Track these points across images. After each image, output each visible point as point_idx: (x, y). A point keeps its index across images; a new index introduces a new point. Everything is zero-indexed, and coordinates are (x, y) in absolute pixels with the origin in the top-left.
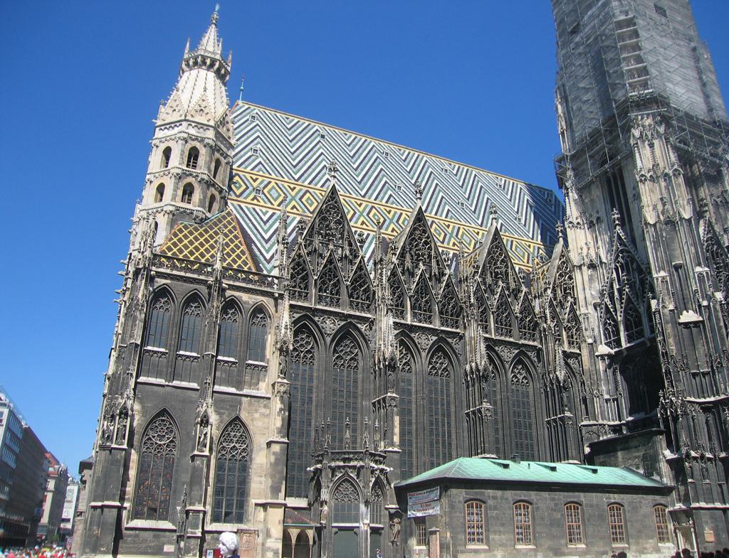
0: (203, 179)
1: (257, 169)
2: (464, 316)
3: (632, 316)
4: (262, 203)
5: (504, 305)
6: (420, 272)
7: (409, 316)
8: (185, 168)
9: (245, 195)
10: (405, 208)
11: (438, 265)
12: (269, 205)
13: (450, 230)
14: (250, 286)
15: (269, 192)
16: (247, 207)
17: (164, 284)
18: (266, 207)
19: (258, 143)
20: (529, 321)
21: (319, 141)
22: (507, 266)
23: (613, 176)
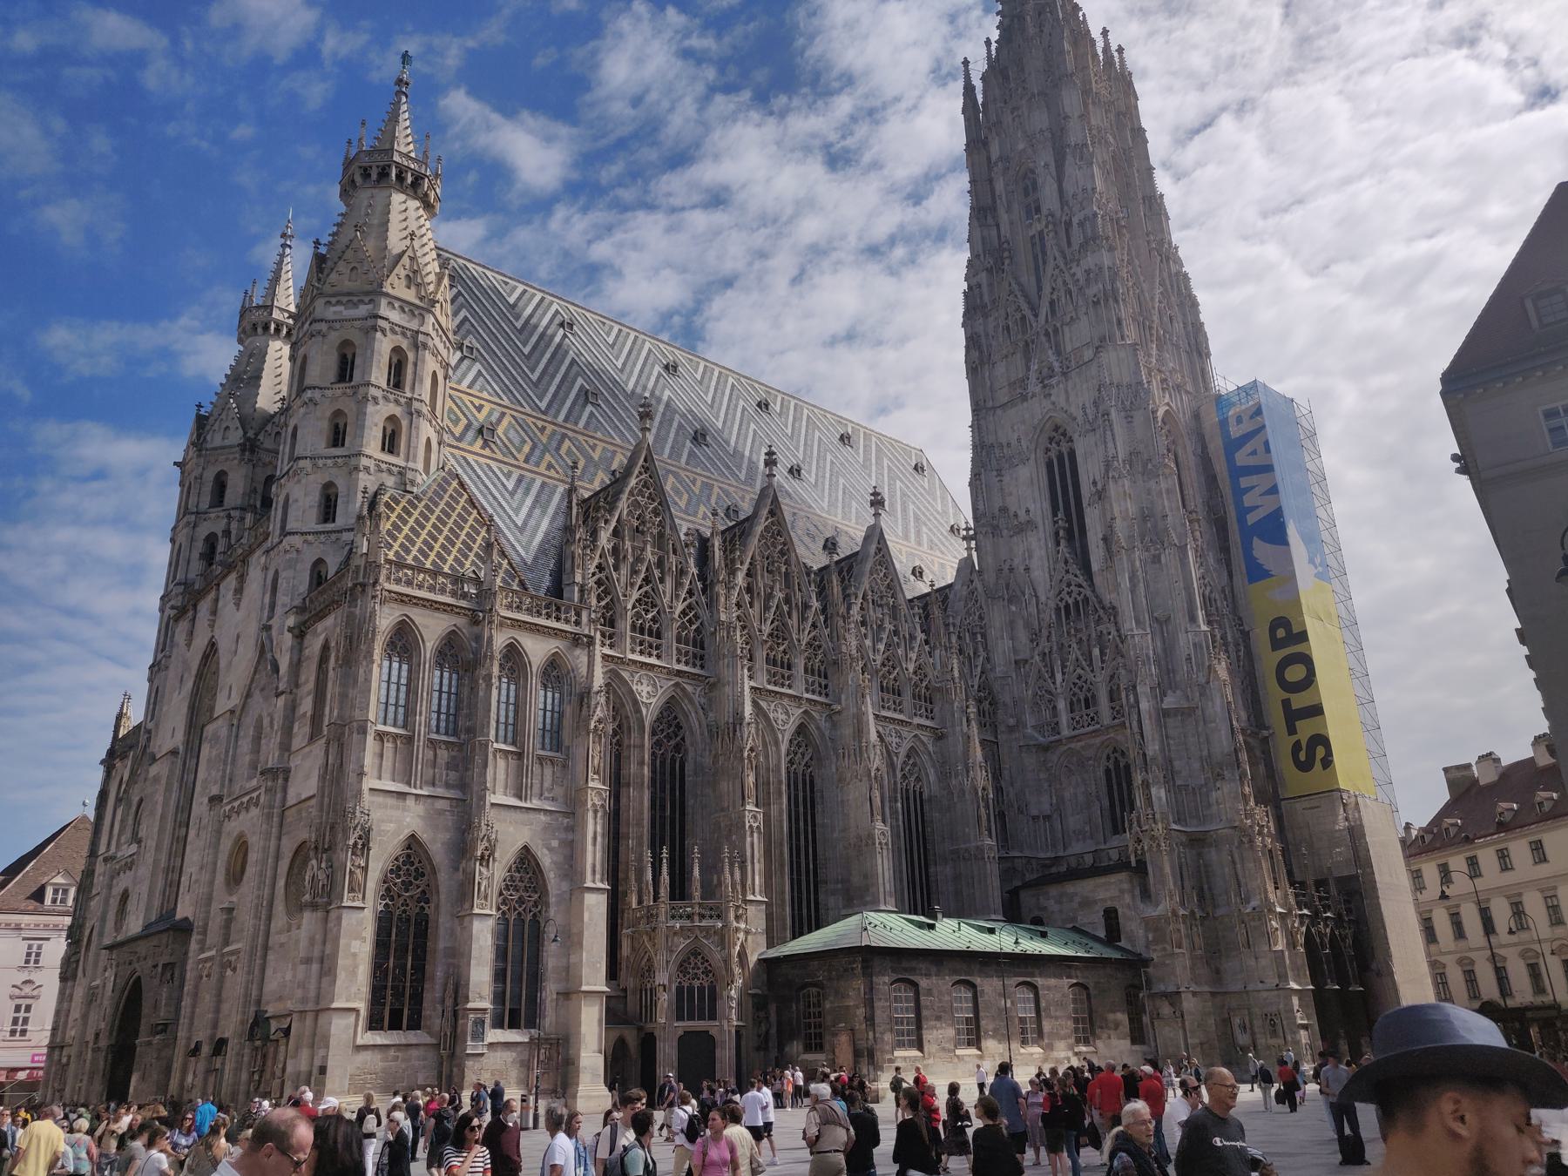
0: (419, 413)
1: (477, 386)
3: (1081, 688)
4: (500, 457)
8: (384, 386)
12: (513, 461)
16: (476, 462)
18: (505, 463)
19: (469, 332)
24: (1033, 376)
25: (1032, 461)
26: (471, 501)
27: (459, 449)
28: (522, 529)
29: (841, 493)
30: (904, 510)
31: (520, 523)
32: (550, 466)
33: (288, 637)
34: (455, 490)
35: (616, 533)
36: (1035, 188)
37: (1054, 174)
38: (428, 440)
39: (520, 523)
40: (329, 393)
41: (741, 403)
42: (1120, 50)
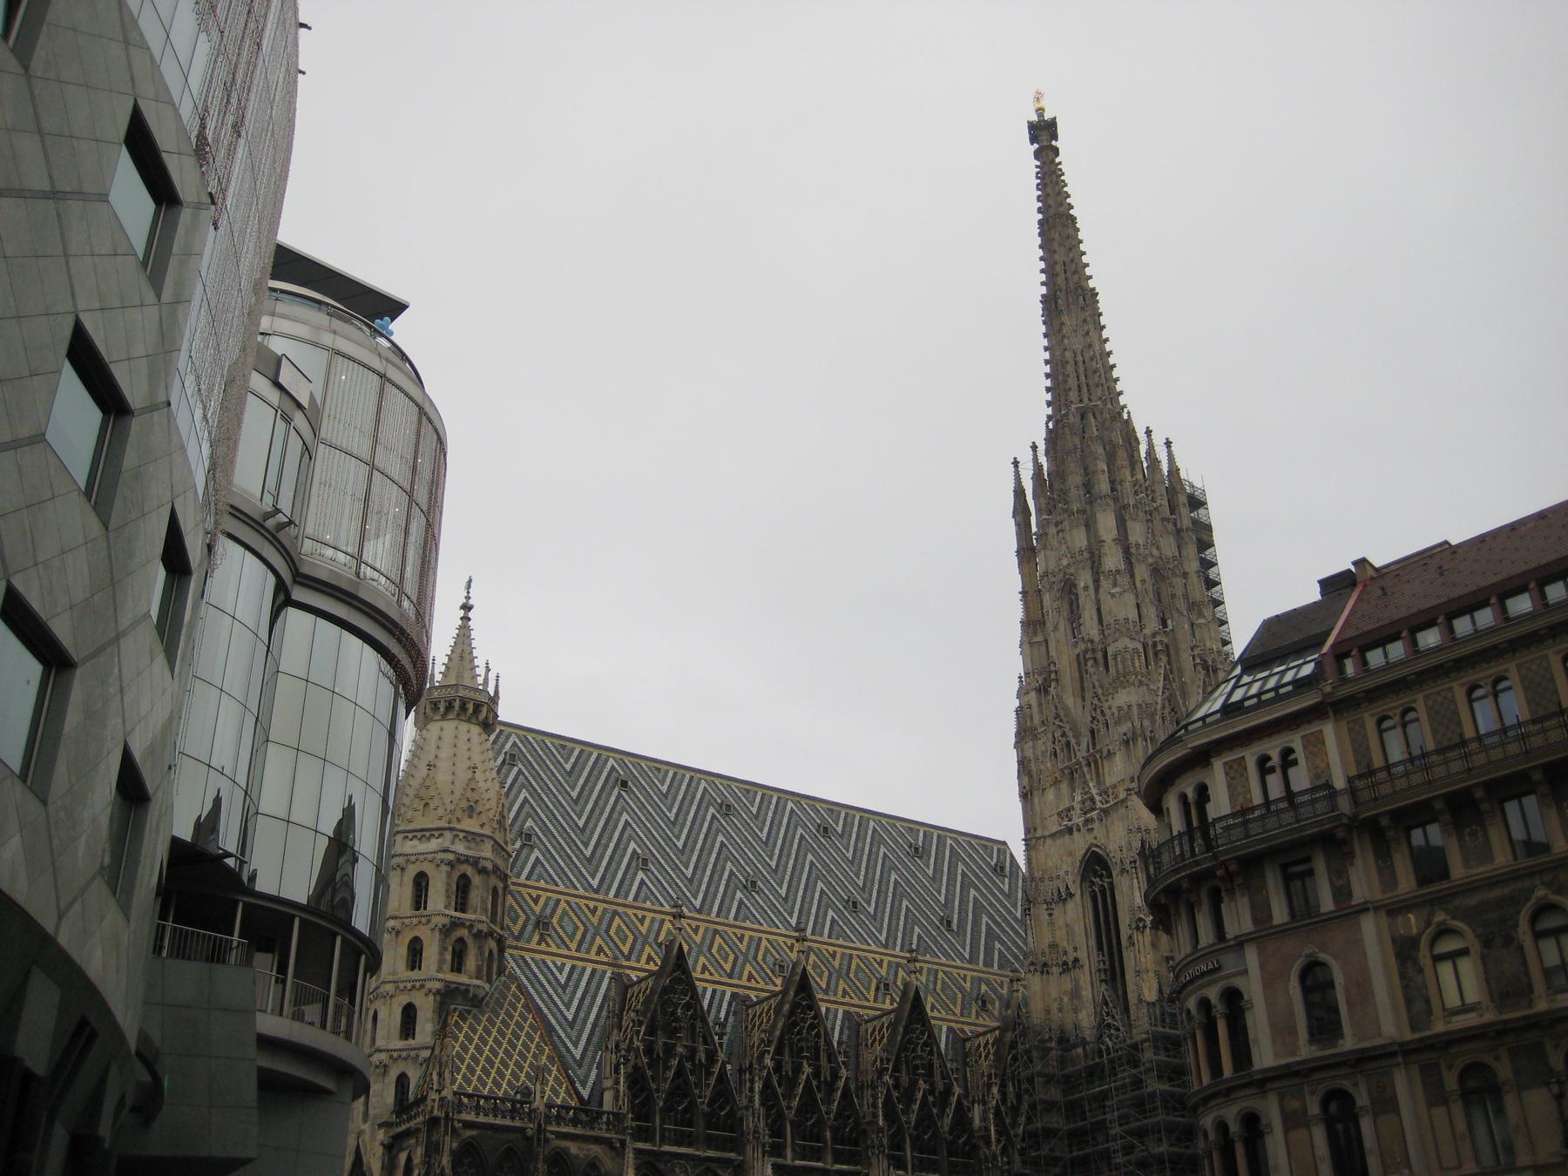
0: (480, 932)
1: (535, 877)
2: (867, 1147)
4: (554, 949)
5: (926, 1120)
6: (804, 1077)
7: (789, 1152)
9: (526, 935)
10: (765, 927)
11: (830, 1061)
13: (836, 963)
14: (579, 1131)
15: (559, 923)
16: (532, 959)
17: (469, 1137)
19: (528, 816)
20: (965, 1143)
21: (619, 796)
22: (931, 1053)
23: (1100, 891)
24: (1077, 806)
25: (1078, 897)
26: (531, 1006)
27: (516, 948)
28: (572, 1024)
29: (902, 918)
30: (976, 922)
31: (570, 1018)
32: (600, 950)
33: (379, 1151)
34: (514, 995)
35: (651, 1031)
36: (1078, 607)
37: (1093, 597)
38: (491, 952)
39: (570, 1018)
40: (407, 921)
41: (800, 831)
42: (1168, 444)
